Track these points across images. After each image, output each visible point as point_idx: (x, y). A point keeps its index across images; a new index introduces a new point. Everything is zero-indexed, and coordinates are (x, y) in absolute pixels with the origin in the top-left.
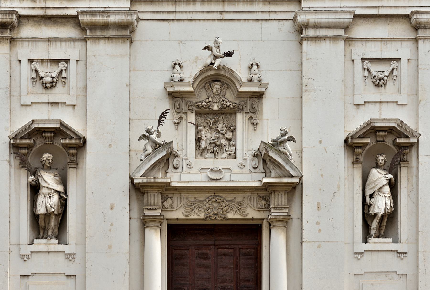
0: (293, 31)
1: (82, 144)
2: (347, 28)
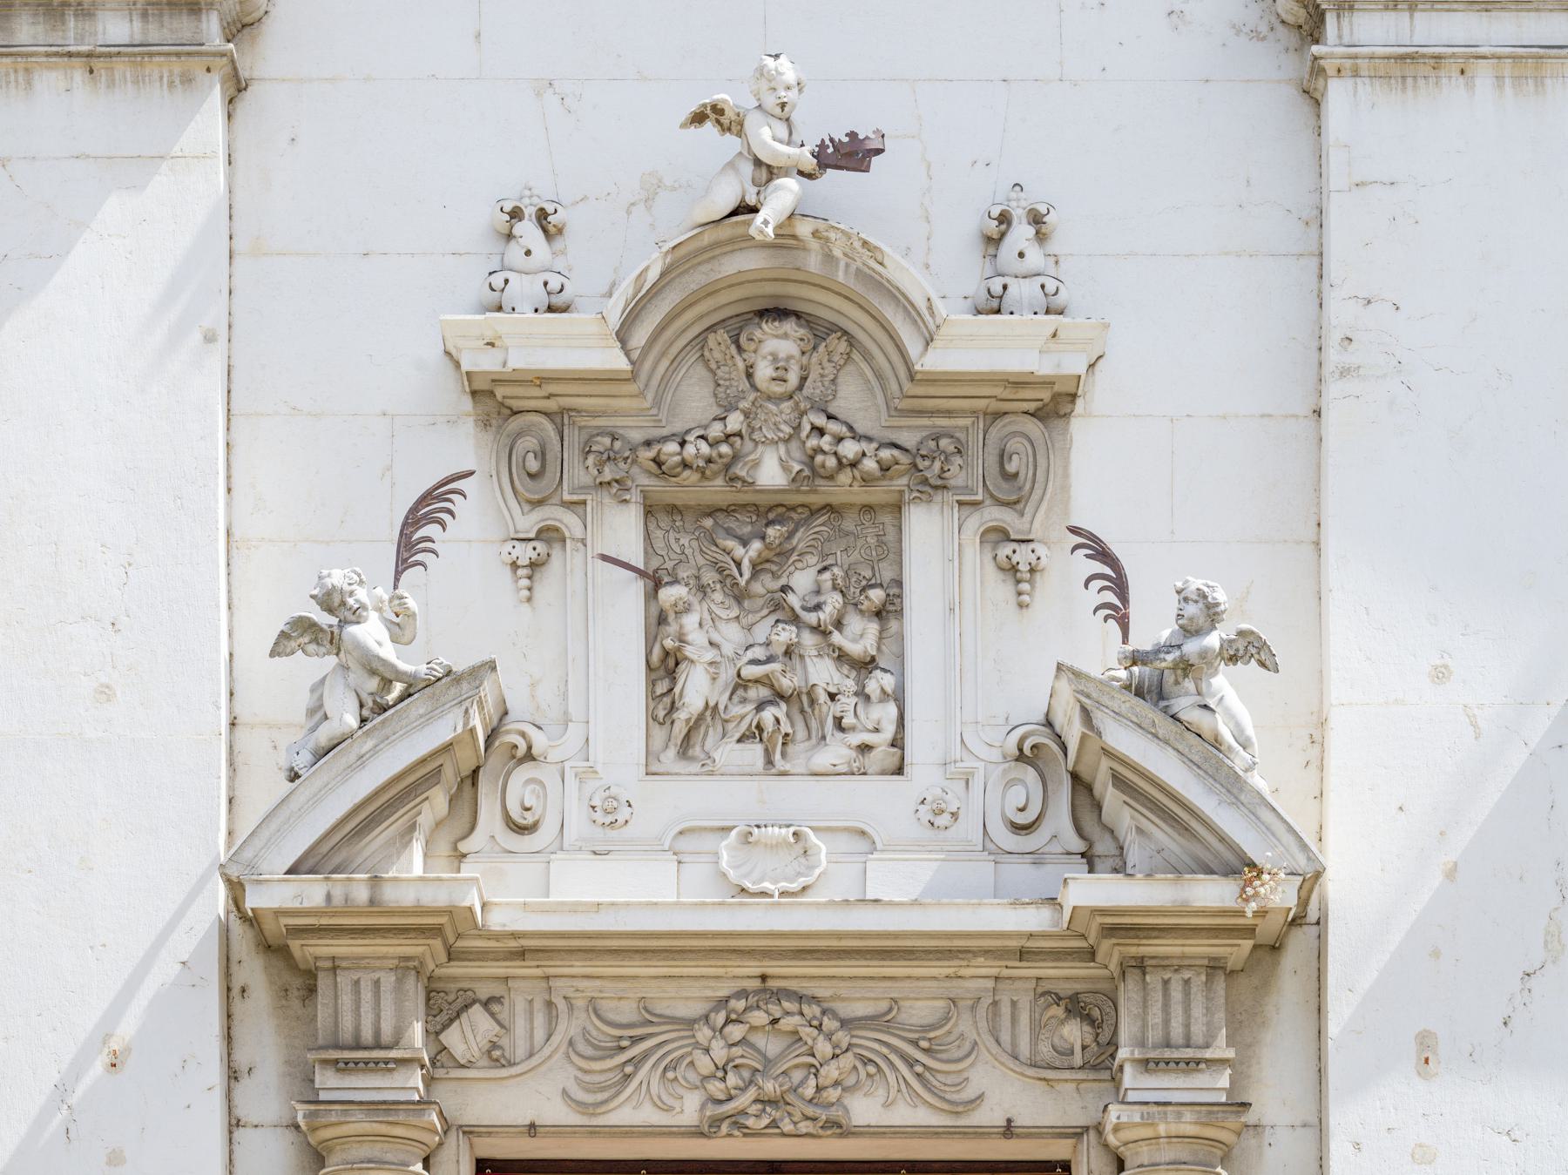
0: (1264, 29)
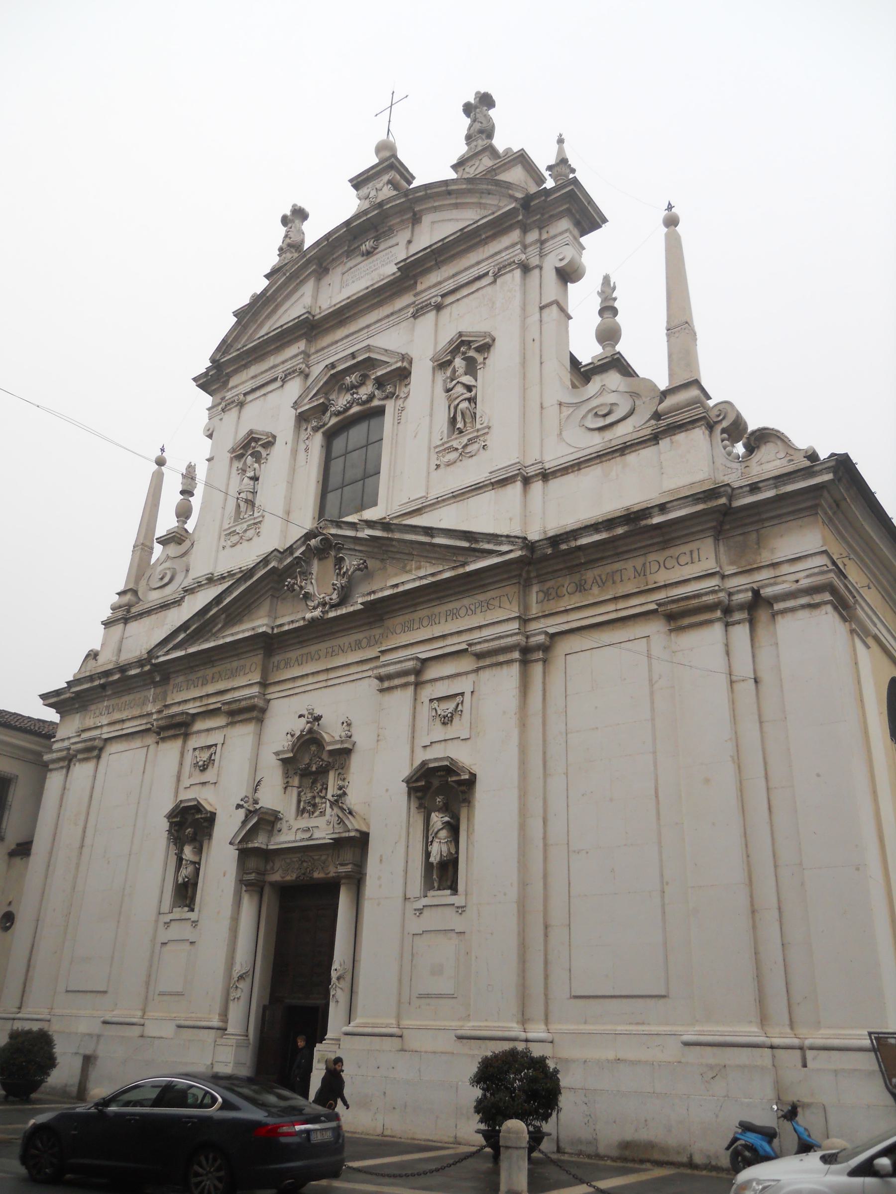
1: (211, 818)
2: (418, 672)
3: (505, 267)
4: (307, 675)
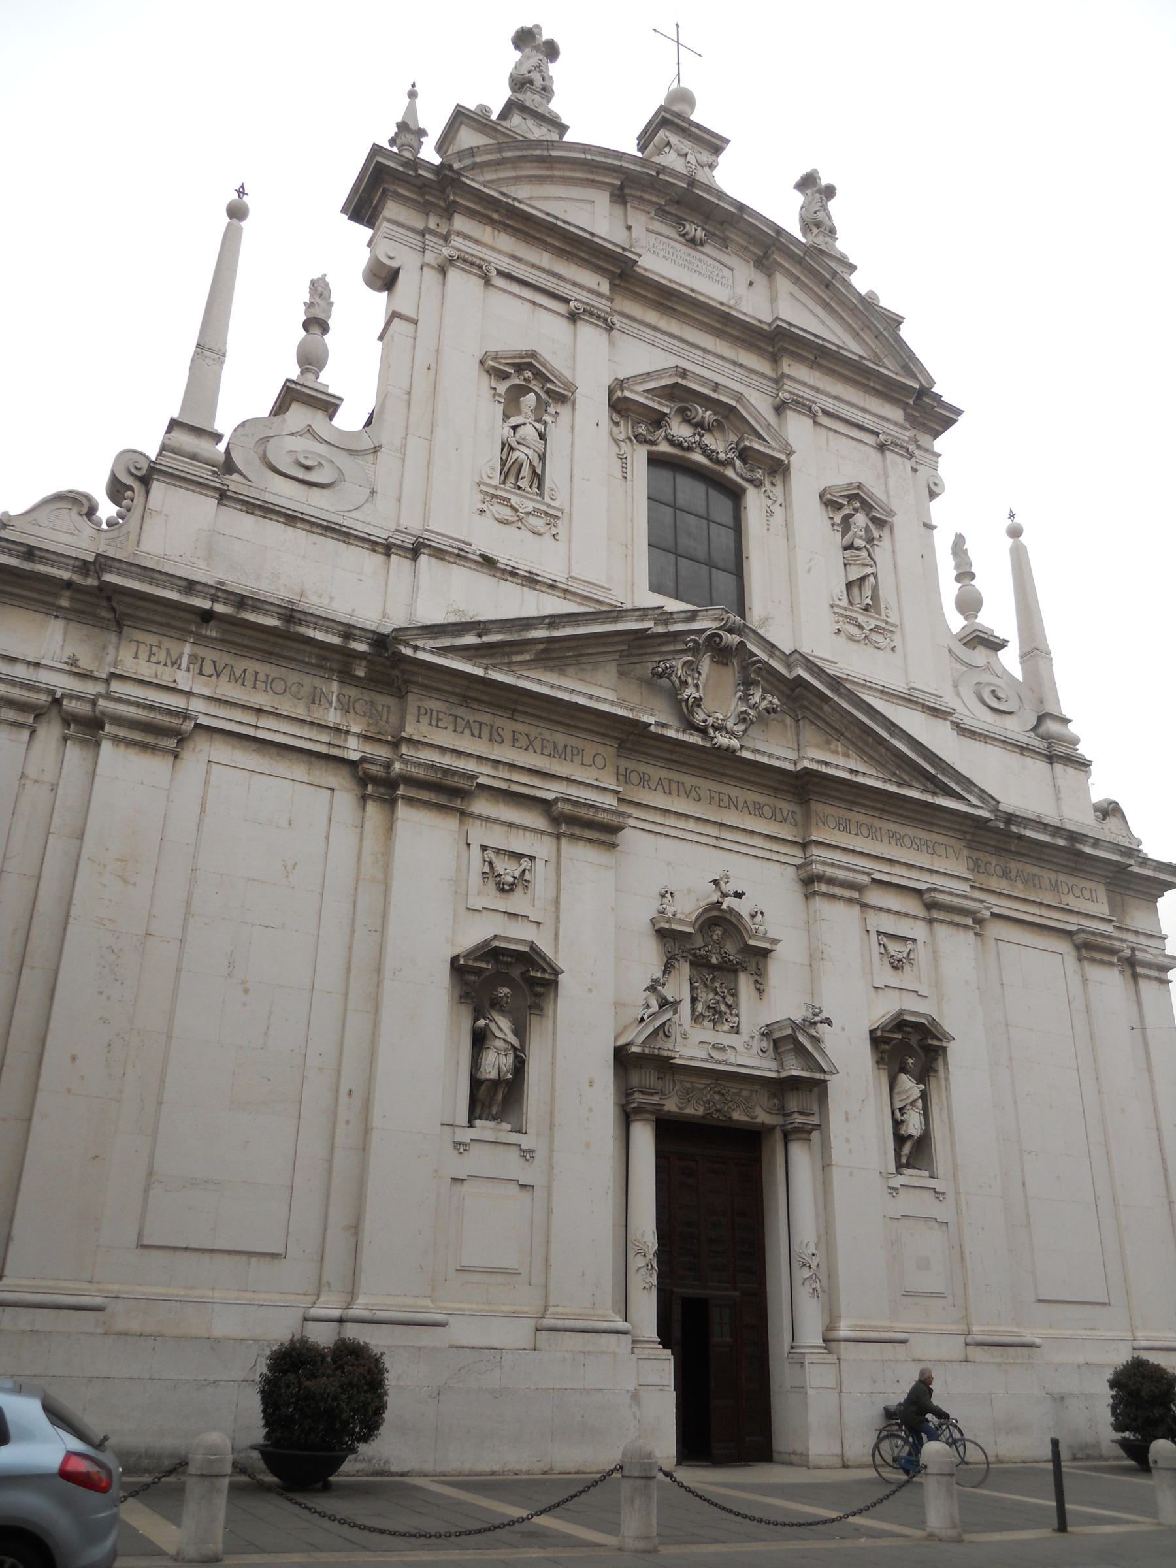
3: (896, 445)
4: (1093, 917)
